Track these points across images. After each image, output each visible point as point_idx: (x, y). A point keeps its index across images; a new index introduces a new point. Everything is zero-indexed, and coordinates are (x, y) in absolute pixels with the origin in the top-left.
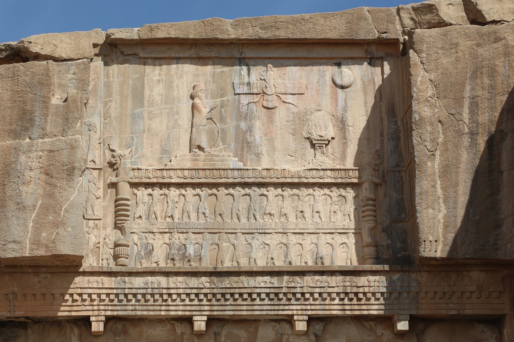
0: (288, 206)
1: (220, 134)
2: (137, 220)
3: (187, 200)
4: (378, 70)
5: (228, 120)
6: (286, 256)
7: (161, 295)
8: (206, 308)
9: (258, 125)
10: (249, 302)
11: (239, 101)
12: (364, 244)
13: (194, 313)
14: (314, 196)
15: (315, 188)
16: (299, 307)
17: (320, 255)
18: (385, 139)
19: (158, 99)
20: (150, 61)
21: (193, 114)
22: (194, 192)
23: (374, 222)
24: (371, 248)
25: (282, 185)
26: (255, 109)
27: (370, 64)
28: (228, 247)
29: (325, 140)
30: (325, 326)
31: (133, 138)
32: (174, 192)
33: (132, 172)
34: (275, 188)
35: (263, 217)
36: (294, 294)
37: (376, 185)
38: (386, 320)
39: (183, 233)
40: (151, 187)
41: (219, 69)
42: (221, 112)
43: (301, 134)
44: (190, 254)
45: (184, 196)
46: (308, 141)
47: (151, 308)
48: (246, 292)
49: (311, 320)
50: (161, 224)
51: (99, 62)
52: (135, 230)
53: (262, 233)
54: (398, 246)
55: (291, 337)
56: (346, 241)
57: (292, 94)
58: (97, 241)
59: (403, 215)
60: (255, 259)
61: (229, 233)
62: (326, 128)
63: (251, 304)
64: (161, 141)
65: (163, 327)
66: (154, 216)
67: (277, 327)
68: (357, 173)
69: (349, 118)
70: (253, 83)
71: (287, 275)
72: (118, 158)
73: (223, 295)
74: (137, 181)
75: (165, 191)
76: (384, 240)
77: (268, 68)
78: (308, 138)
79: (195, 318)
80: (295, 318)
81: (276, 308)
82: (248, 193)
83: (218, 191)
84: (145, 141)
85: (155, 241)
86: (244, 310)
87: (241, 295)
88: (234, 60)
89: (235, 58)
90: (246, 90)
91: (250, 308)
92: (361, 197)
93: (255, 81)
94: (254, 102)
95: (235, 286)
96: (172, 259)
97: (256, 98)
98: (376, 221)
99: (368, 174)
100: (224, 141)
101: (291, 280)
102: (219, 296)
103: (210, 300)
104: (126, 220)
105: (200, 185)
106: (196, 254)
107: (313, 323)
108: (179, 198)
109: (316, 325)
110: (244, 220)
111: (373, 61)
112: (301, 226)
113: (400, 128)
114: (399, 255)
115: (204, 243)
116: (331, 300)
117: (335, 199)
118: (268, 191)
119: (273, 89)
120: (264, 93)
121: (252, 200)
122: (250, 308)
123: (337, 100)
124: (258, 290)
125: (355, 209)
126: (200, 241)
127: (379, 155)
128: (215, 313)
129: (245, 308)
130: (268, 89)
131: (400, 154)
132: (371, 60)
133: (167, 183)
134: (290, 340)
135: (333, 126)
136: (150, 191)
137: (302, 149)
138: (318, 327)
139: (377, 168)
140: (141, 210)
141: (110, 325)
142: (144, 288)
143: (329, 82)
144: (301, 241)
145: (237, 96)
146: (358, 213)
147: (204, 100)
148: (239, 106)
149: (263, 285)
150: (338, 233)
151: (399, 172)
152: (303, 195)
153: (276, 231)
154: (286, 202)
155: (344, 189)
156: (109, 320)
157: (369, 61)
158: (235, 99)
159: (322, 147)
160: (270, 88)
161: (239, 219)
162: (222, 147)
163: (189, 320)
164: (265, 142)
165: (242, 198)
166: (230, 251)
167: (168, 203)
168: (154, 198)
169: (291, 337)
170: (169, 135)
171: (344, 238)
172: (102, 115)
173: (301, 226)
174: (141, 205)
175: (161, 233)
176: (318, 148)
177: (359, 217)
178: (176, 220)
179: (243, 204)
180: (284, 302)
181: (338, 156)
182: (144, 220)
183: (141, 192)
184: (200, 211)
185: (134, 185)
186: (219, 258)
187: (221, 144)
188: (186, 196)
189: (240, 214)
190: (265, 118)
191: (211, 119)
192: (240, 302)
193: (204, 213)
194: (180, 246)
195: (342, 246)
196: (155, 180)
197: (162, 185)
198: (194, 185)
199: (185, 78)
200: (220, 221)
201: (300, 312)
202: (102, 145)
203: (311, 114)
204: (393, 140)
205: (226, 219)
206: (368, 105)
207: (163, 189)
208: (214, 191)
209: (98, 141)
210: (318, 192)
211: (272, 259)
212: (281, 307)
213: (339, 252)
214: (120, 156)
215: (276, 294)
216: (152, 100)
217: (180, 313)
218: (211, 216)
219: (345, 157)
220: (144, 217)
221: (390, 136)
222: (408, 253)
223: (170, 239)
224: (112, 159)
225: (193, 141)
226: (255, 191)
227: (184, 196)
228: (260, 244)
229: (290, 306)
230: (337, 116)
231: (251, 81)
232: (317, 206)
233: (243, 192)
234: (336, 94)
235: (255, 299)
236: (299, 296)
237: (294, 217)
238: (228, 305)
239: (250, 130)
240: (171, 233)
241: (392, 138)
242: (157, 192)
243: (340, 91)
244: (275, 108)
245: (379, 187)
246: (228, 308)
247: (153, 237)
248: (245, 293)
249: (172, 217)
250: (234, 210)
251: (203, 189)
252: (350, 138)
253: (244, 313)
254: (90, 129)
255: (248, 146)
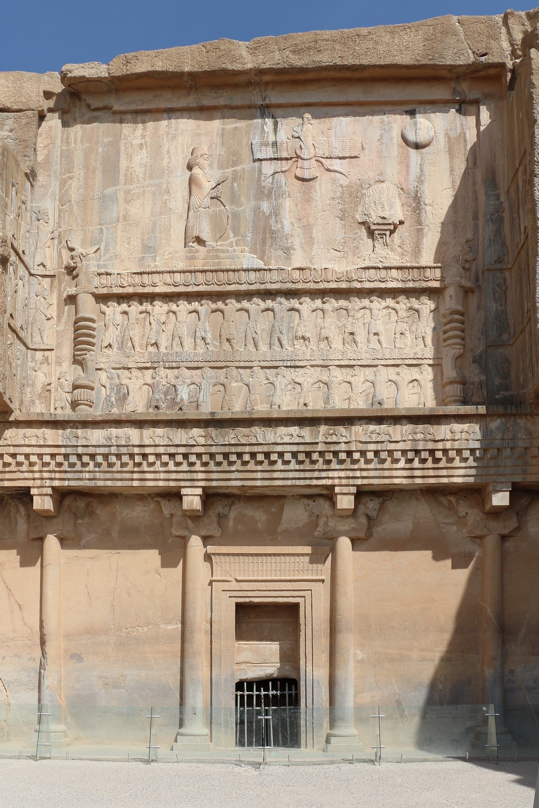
0: (331, 325)
1: (230, 221)
2: (106, 350)
3: (179, 319)
4: (472, 120)
5: (242, 199)
6: (327, 401)
7: (132, 456)
8: (201, 476)
9: (287, 204)
10: (266, 466)
11: (260, 171)
12: (445, 380)
13: (182, 484)
14: (370, 309)
15: (373, 298)
17: (378, 398)
18: (481, 223)
19: (139, 171)
20: (129, 116)
21: (190, 192)
22: (191, 307)
23: (462, 347)
24: (455, 386)
25: (323, 294)
26: (283, 182)
27: (459, 111)
28: (241, 388)
29: (390, 224)
30: (383, 503)
31: (101, 230)
32: (159, 308)
33: (97, 278)
34: (313, 300)
35: (293, 342)
37: (467, 292)
38: (475, 493)
39: (173, 368)
40: (126, 301)
41: (232, 124)
42: (232, 188)
43: (353, 218)
44: (182, 400)
45: (174, 313)
46: (363, 227)
47: (119, 476)
49: (362, 494)
50: (141, 355)
51: (53, 122)
52: (102, 366)
53: (291, 367)
54: (497, 383)
55: (331, 519)
56: (418, 377)
57: (340, 158)
58: (47, 381)
59: (505, 337)
60: (279, 406)
61: (241, 367)
62: (391, 206)
64: (142, 234)
66: (130, 344)
67: (311, 506)
68: (438, 273)
69: (426, 192)
70: (282, 143)
72: (78, 259)
73: (226, 456)
74: (105, 291)
75: (147, 306)
76: (475, 375)
77: (305, 119)
78: (363, 223)
79: (184, 491)
81: (308, 474)
82: (270, 307)
83: (226, 305)
84: (119, 234)
85: (131, 381)
86: (257, 479)
87: (253, 455)
88: (253, 111)
89: (255, 107)
90: (269, 152)
92: (442, 311)
93: (285, 140)
94: (282, 172)
95: (244, 442)
96: (156, 407)
97: (285, 165)
98: (464, 346)
99: (455, 275)
100: (236, 232)
102: (219, 458)
103: (206, 464)
104: (89, 350)
105: (199, 296)
106: (192, 400)
107: (365, 499)
108: (168, 317)
109: (370, 502)
110: (263, 347)
111: (464, 106)
112: (350, 355)
113: (504, 205)
114: (497, 397)
115: (204, 382)
116: (392, 463)
117: (403, 313)
118: (301, 304)
119: (312, 150)
120: (298, 157)
121: (277, 316)
123: (408, 166)
125: (434, 329)
126: (197, 380)
127: (471, 245)
128: (214, 484)
129: (259, 475)
130: (305, 150)
131: (504, 244)
132: (460, 105)
133: (148, 293)
134: (330, 524)
135: (403, 205)
136: (124, 306)
137: (355, 239)
138: (372, 505)
139: (467, 266)
140: (111, 336)
141: (67, 502)
142: (105, 446)
143: (397, 139)
144: (349, 378)
145: (257, 164)
146: (437, 334)
147: (207, 170)
148: (259, 179)
150: (407, 365)
151: (501, 270)
152: (354, 309)
153: (312, 363)
154: (328, 320)
155: (418, 298)
156: (61, 495)
157: (457, 106)
158: (253, 168)
159: (385, 234)
160: (307, 148)
161: (256, 346)
162: (234, 240)
163: (174, 495)
164: (299, 231)
165: (262, 315)
166: (242, 394)
167: (150, 324)
168: (130, 316)
169: (331, 519)
170: (154, 224)
171: (414, 373)
172: (57, 197)
173: (351, 355)
174: (111, 329)
175: (140, 369)
176: (378, 237)
177: (438, 340)
178: (163, 349)
179: (263, 324)
181: (409, 250)
182: (115, 350)
183: (111, 308)
184: (198, 334)
185: (102, 298)
186: (225, 405)
187: (232, 235)
188: (178, 313)
189: (259, 338)
190: (299, 195)
191: (217, 198)
192: (251, 466)
193: (203, 339)
194: (168, 388)
195: (411, 384)
196: (131, 290)
197: (142, 298)
198: (189, 297)
199: (180, 140)
200: (227, 350)
202: (56, 241)
203: (369, 187)
204: (493, 223)
205: (236, 347)
206: (455, 173)
207: (145, 304)
208: (220, 304)
209: (49, 236)
210: (377, 304)
211: (305, 405)
213: (407, 394)
214: (82, 256)
216: (131, 174)
218: (214, 342)
219: (419, 251)
220: (115, 346)
221: (489, 216)
222: (510, 393)
223: (154, 378)
224: (71, 262)
225: (189, 232)
226: (281, 304)
227: (174, 313)
228: (287, 382)
230: (408, 189)
231: (278, 140)
232: (376, 324)
233: (263, 305)
234: (408, 156)
235: (274, 462)
237: (340, 342)
238: (233, 471)
239: (276, 212)
240: (155, 368)
241: (492, 220)
242: (135, 308)
243: (413, 152)
244: (314, 179)
245: (470, 294)
247: (129, 375)
249: (157, 346)
250: (249, 332)
251: (203, 302)
252: (427, 222)
253: (259, 483)
254: (39, 218)
255: (272, 237)
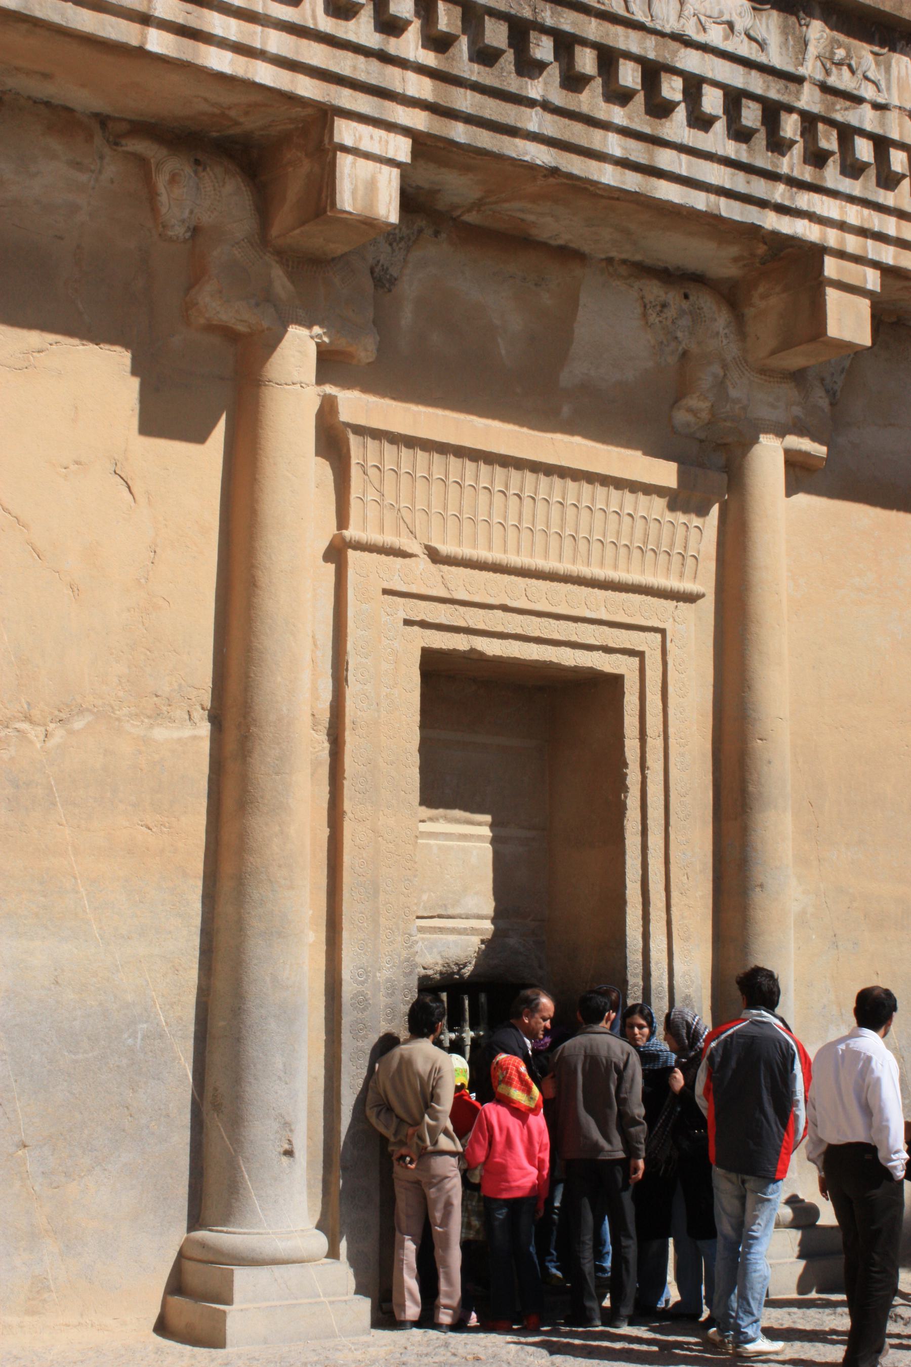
13: (346, 98)
16: (854, 215)
36: (847, 133)
48: (635, 49)
63: (647, 130)
65: (77, 165)
67: (671, 313)
71: (826, 22)
79: (346, 132)
80: (831, 267)
87: (608, 58)
91: (637, 152)
101: (840, 53)
122: (637, 152)
124: (691, 61)
128: (460, 132)
129: (614, 145)
134: (734, 393)
149: (715, 36)
180: (791, 163)
192: (590, 100)
201: (852, 244)
212: (779, 193)
215: (772, 112)
217: (265, 74)
229: (816, 197)
236: (864, 150)
238: (531, 103)
246: (534, 120)
248: (628, 56)
253: (608, 175)
